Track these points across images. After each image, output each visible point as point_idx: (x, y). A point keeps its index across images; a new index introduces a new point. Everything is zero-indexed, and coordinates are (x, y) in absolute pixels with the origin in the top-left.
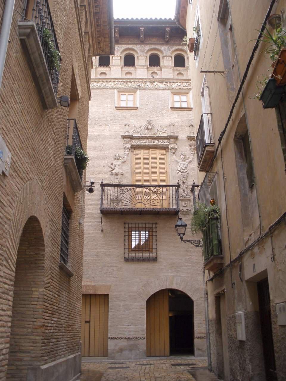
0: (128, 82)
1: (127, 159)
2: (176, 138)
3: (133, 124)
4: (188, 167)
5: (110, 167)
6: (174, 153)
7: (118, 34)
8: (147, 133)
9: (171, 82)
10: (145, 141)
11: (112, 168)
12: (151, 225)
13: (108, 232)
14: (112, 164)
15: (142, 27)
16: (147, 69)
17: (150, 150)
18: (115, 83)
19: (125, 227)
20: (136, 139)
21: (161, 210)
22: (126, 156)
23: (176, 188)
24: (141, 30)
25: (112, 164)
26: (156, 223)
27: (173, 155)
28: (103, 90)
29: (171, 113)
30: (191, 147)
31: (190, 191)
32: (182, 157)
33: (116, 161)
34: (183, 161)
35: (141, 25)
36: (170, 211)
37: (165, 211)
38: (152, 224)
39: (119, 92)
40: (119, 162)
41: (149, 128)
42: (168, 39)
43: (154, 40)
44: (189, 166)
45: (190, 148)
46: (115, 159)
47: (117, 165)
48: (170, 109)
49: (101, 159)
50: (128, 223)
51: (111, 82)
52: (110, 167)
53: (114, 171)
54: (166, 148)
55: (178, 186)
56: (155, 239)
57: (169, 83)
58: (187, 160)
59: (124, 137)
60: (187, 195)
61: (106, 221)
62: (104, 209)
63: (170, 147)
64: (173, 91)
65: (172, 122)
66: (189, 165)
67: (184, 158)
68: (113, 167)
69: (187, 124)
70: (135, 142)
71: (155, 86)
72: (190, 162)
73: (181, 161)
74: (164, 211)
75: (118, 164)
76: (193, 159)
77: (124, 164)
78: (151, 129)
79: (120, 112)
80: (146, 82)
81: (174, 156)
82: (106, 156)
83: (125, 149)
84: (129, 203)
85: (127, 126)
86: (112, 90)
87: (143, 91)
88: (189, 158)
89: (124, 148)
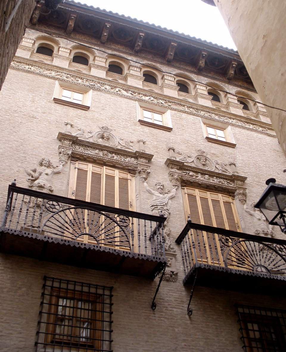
0: (77, 77)
1: (62, 170)
2: (149, 158)
3: (78, 126)
4: (169, 204)
5: (29, 175)
6: (146, 179)
7: (73, 23)
8: (100, 142)
9: (139, 94)
10: (97, 151)
11: (32, 177)
12: (100, 292)
13: (5, 290)
14: (35, 171)
15: (108, 22)
16: (107, 72)
17: (104, 167)
18: (59, 73)
19: (44, 286)
20: (83, 145)
21: (131, 256)
22: (61, 166)
23: (158, 223)
24: (106, 25)
25: (35, 171)
26: (111, 289)
27: (143, 182)
28: (38, 76)
29: (140, 127)
30: (172, 176)
31: (174, 241)
32: (158, 187)
33: (43, 167)
34: (161, 194)
35: (107, 20)
36: (147, 260)
37: (138, 258)
38: (104, 288)
39: (61, 86)
40: (49, 171)
41: (105, 135)
42: (138, 48)
43: (119, 46)
44: (171, 204)
45: (171, 177)
46: (41, 165)
47: (43, 174)
48: (139, 123)
49: (16, 160)
50: (53, 280)
51: (52, 70)
52: (29, 175)
53: (36, 182)
54: (132, 171)
55: (161, 220)
56: (108, 320)
57: (137, 94)
58: (167, 193)
59: (62, 137)
60: (169, 247)
61: (5, 267)
62: (9, 232)
63: (139, 168)
64: (144, 105)
65: (142, 139)
66: (170, 201)
67: (162, 190)
68: (36, 175)
69: (165, 147)
70: (80, 150)
71: (117, 92)
72: (172, 198)
73: (157, 193)
74: (136, 257)
75: (46, 172)
76: (176, 194)
77: (56, 176)
78: (108, 139)
79: (59, 107)
80: (103, 84)
81: (145, 184)
82: (25, 157)
83: (61, 155)
84: (70, 228)
85: (69, 126)
86: (52, 80)
87: (99, 93)
88: (169, 191)
89: (60, 153)
